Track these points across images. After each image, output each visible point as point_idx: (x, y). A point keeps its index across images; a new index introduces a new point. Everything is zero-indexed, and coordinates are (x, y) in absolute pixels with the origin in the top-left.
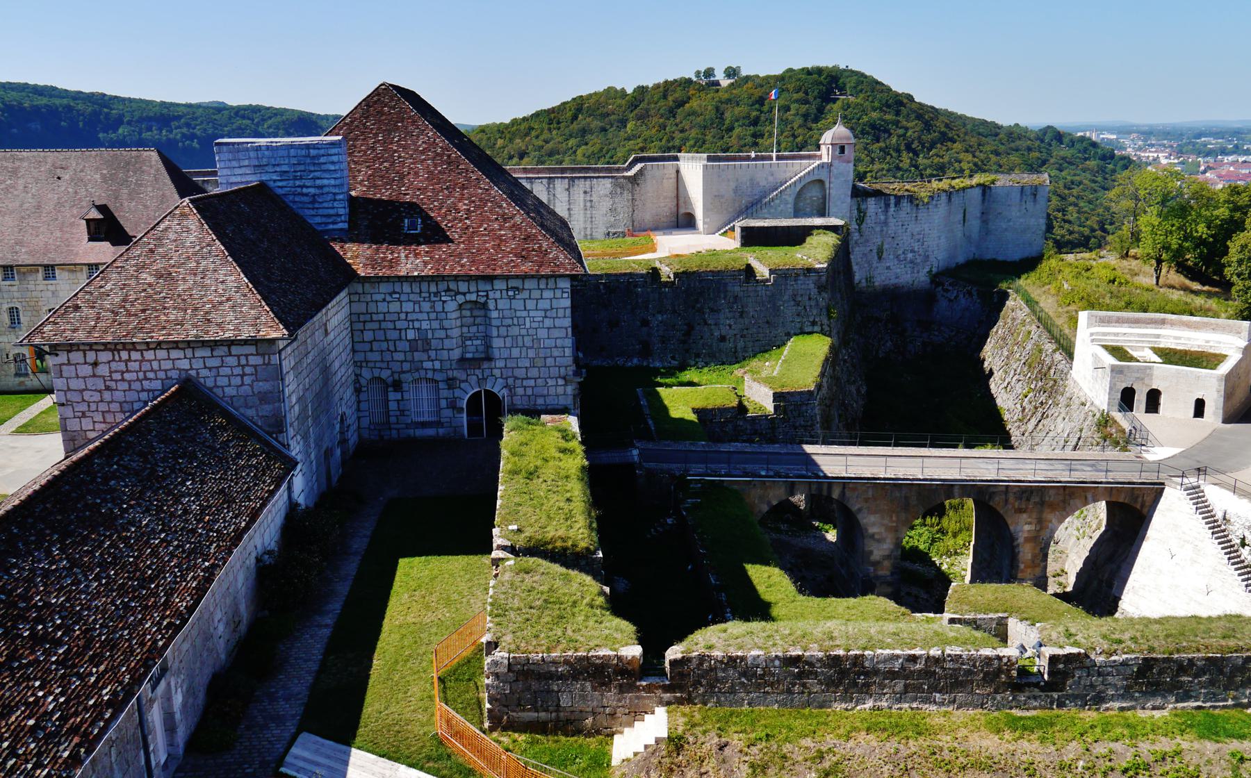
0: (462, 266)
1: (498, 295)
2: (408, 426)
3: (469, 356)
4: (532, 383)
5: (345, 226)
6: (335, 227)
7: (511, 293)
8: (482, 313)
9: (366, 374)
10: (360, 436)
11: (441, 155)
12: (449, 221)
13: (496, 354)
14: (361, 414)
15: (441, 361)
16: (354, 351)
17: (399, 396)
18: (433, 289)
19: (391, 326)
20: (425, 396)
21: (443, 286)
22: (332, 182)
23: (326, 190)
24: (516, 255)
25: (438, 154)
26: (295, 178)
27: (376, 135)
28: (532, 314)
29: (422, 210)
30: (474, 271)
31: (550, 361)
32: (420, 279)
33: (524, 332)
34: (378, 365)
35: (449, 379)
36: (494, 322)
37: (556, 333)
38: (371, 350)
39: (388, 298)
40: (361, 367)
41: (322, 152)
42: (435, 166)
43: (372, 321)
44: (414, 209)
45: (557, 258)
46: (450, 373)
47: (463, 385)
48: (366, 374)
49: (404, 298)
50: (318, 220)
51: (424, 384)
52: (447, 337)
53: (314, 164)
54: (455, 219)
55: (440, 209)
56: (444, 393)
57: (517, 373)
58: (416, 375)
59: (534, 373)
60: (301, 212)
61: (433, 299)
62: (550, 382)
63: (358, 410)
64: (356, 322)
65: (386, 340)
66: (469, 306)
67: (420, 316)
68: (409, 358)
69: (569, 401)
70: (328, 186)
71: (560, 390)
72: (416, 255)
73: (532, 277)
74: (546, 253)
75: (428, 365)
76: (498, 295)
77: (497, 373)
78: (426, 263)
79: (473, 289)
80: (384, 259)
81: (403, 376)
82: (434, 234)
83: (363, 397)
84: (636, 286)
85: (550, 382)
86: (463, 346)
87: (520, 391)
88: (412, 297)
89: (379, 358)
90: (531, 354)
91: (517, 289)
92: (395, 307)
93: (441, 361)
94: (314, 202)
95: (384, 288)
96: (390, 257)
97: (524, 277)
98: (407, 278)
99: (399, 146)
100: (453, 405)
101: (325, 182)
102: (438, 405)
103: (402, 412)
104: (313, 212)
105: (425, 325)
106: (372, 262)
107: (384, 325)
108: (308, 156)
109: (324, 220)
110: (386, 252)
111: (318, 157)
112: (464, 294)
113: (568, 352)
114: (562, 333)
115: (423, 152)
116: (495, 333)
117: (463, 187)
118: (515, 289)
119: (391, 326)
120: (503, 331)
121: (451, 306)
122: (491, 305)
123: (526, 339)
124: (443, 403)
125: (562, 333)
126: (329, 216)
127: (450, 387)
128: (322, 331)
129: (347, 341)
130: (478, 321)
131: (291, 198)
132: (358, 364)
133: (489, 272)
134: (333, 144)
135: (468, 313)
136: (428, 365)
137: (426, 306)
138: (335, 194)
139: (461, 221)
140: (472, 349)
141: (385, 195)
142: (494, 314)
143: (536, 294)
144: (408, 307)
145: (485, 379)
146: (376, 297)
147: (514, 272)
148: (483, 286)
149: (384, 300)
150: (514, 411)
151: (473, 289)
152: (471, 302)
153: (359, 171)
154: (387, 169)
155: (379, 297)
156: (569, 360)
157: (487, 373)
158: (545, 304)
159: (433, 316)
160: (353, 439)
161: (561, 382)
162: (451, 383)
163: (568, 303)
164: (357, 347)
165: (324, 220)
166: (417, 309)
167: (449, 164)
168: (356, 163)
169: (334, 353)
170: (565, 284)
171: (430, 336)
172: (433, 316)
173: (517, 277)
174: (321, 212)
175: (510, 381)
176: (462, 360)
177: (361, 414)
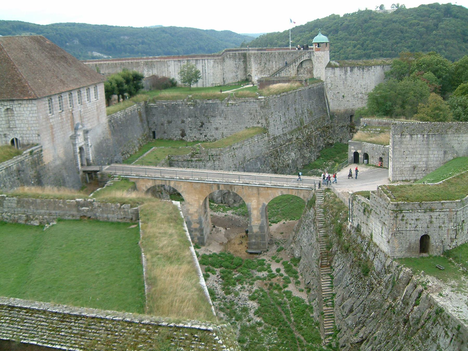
4: (28, 136)
33: (24, 118)
36: (16, 115)
47: (9, 136)
57: (24, 132)
62: (34, 135)
76: (15, 106)
77: (18, 132)
79: (8, 104)
87: (25, 138)
118: (20, 104)
121: (3, 110)
122: (14, 109)
127: (5, 137)
142: (15, 113)
143: (26, 106)
158: (29, 109)
161: (37, 135)
175: (22, 135)
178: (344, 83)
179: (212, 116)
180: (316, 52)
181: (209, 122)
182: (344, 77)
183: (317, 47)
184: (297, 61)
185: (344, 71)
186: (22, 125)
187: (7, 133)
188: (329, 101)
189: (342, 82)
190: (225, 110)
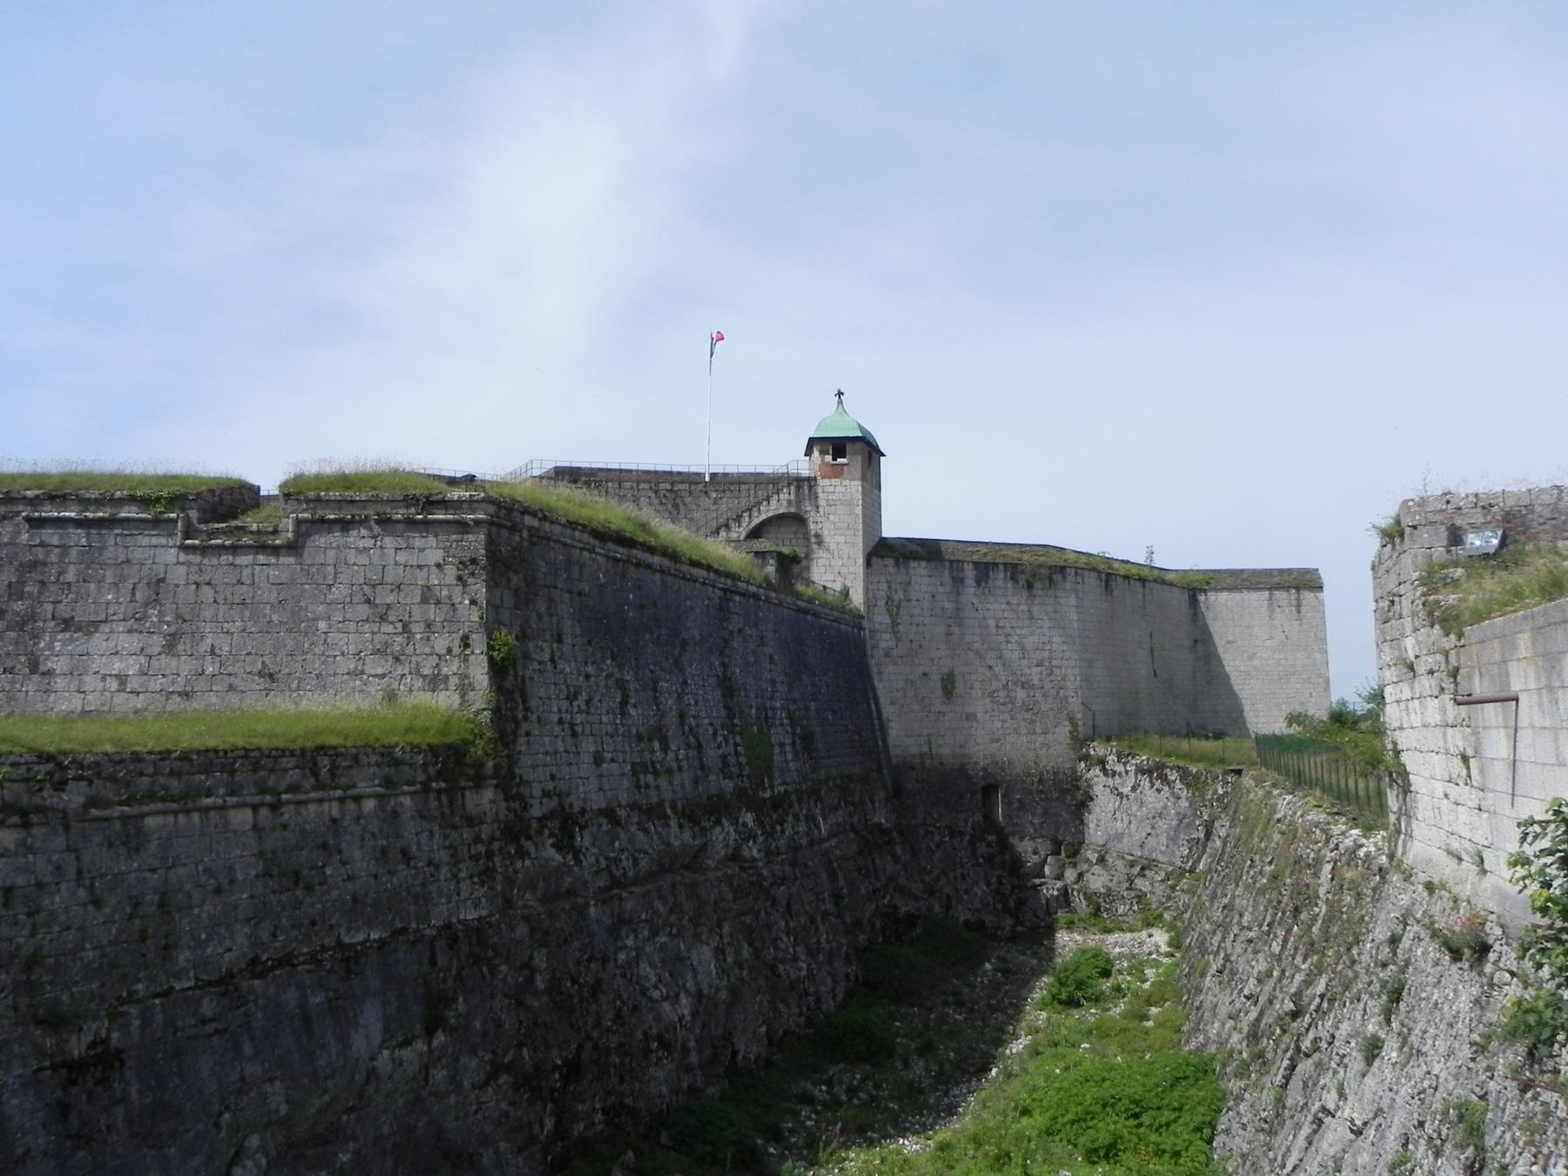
178: (949, 634)
179: (67, 624)
180: (826, 482)
181: (34, 667)
182: (949, 605)
183: (829, 458)
184: (738, 519)
185: (948, 580)
188: (888, 711)
189: (940, 629)
190: (179, 575)
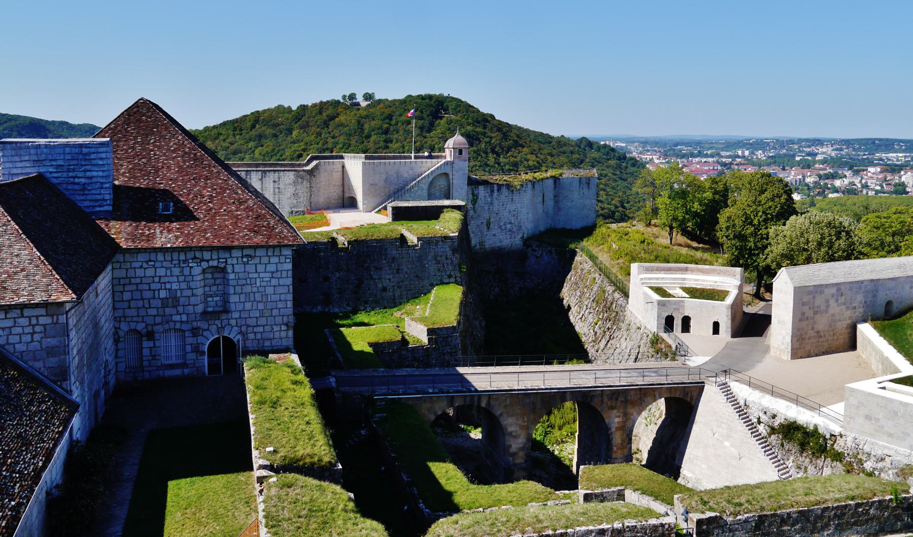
0: (207, 239)
1: (235, 261)
2: (158, 368)
3: (210, 309)
4: (261, 329)
5: (110, 208)
6: (101, 209)
7: (245, 260)
8: (221, 275)
9: (124, 327)
10: (116, 378)
11: (189, 154)
12: (196, 204)
13: (233, 307)
14: (118, 360)
15: (188, 314)
16: (114, 308)
17: (151, 344)
18: (182, 257)
19: (146, 287)
20: (173, 343)
21: (190, 255)
22: (101, 174)
23: (95, 180)
24: (249, 231)
25: (186, 153)
26: (69, 171)
27: (136, 138)
28: (262, 275)
29: (174, 196)
30: (216, 243)
31: (275, 312)
32: (173, 250)
33: (255, 290)
34: (135, 319)
35: (194, 328)
36: (231, 283)
37: (281, 290)
38: (129, 307)
39: (145, 265)
40: (120, 322)
41: (93, 150)
42: (184, 162)
43: (130, 284)
44: (167, 195)
45: (282, 232)
46: (195, 324)
47: (205, 333)
48: (124, 327)
49: (158, 265)
50: (87, 203)
51: (173, 333)
52: (193, 295)
53: (86, 160)
54: (200, 202)
55: (188, 195)
56: (190, 340)
57: (250, 322)
58: (166, 327)
59: (262, 321)
60: (73, 198)
61: (182, 265)
63: (116, 357)
64: (117, 284)
65: (142, 299)
66: (210, 270)
67: (171, 279)
68: (161, 313)
69: (290, 343)
70: (97, 177)
71: (283, 334)
72: (169, 231)
73: (262, 247)
74: (274, 228)
75: (177, 318)
77: (233, 322)
78: (177, 237)
79: (215, 257)
80: (142, 234)
81: (155, 328)
82: (184, 214)
83: (120, 345)
84: (319, 252)
85: (276, 328)
86: (206, 302)
87: (251, 336)
88: (164, 263)
89: (136, 314)
90: (261, 306)
91: (250, 256)
92: (150, 272)
93: (188, 314)
94: (84, 189)
95: (141, 257)
96: (147, 232)
97: (256, 247)
98: (163, 250)
99: (155, 146)
100: (196, 349)
101: (95, 174)
102: (184, 349)
103: (154, 357)
104: (82, 198)
105: (175, 286)
106: (133, 237)
107: (140, 287)
108: (81, 153)
109: (92, 204)
110: (144, 228)
111: (89, 154)
112: (208, 261)
113: (290, 304)
114: (285, 290)
115: (174, 152)
116: (232, 291)
117: (207, 178)
119: (146, 287)
120: (238, 289)
121: (197, 270)
122: (229, 269)
123: (256, 295)
124: (188, 348)
125: (285, 290)
126: (97, 200)
127: (194, 335)
128: (94, 293)
129: (110, 300)
130: (218, 281)
131: (64, 186)
132: (117, 320)
133: (229, 243)
134: (102, 144)
135: (210, 276)
136: (177, 318)
137: (176, 271)
138: (102, 183)
139: (205, 204)
140: (213, 304)
141: (143, 184)
142: (232, 276)
143: (265, 260)
144: (161, 272)
145: (223, 328)
146: (134, 265)
147: (248, 243)
148: (223, 254)
149: (141, 267)
150: (248, 352)
151: (215, 257)
152: (213, 267)
153: (122, 165)
154: (145, 164)
155: (138, 265)
156: (290, 311)
157: (225, 322)
159: (182, 279)
160: (112, 381)
161: (284, 328)
162: (195, 332)
163: (290, 266)
164: (118, 305)
165: (92, 204)
166: (169, 274)
167: (195, 160)
168: (119, 159)
169: (102, 312)
170: (288, 252)
171: (179, 294)
172: (182, 279)
173: (250, 247)
174: (89, 197)
175: (243, 329)
176: (205, 313)
177: (118, 360)
186: (248, 306)
187: (203, 325)
